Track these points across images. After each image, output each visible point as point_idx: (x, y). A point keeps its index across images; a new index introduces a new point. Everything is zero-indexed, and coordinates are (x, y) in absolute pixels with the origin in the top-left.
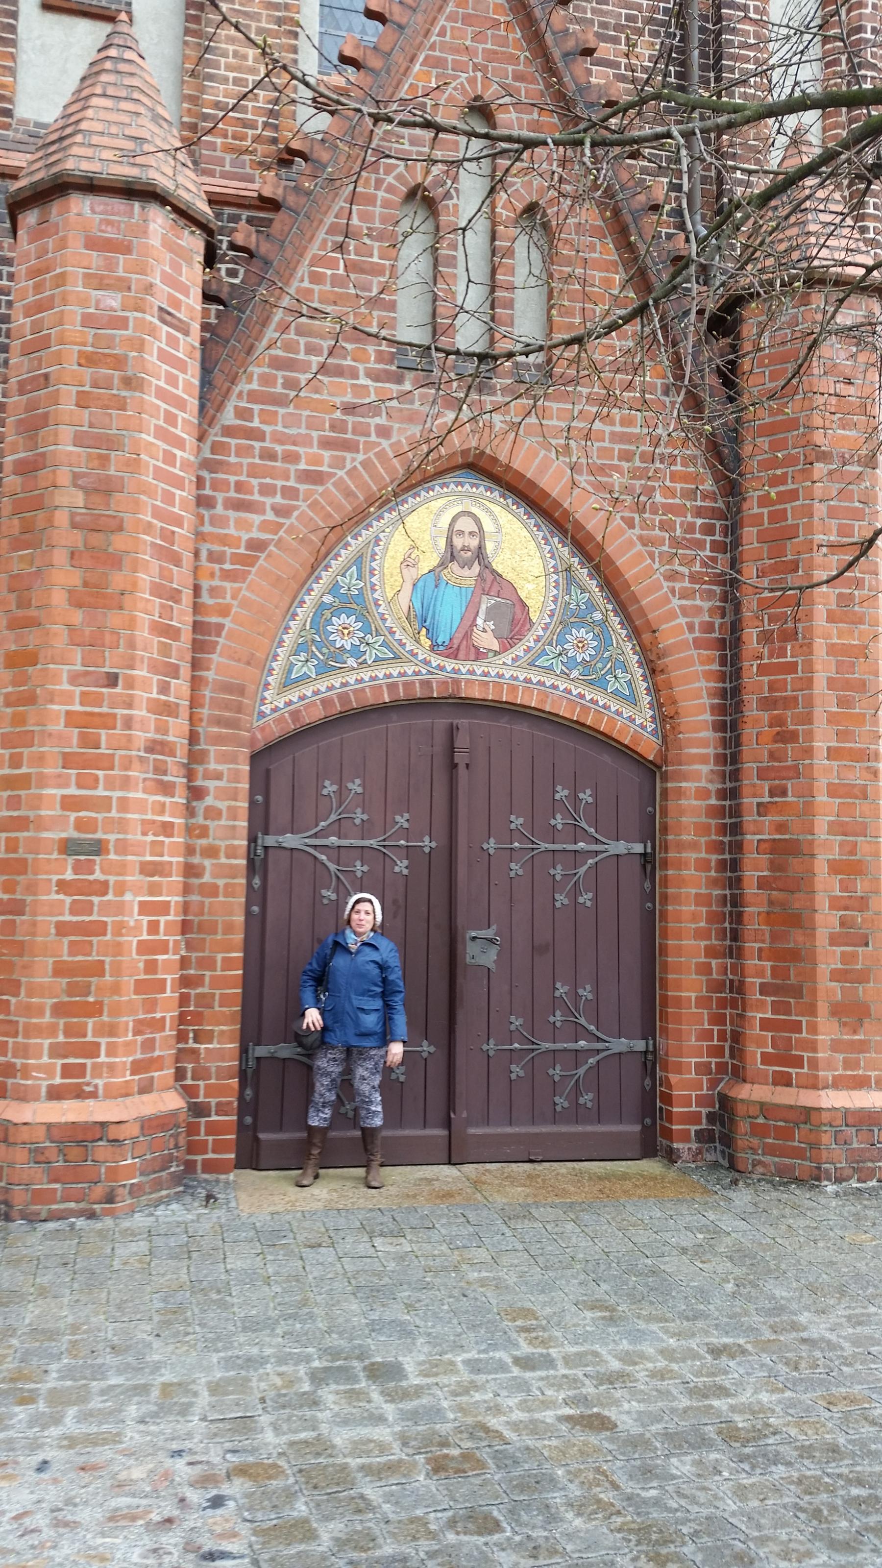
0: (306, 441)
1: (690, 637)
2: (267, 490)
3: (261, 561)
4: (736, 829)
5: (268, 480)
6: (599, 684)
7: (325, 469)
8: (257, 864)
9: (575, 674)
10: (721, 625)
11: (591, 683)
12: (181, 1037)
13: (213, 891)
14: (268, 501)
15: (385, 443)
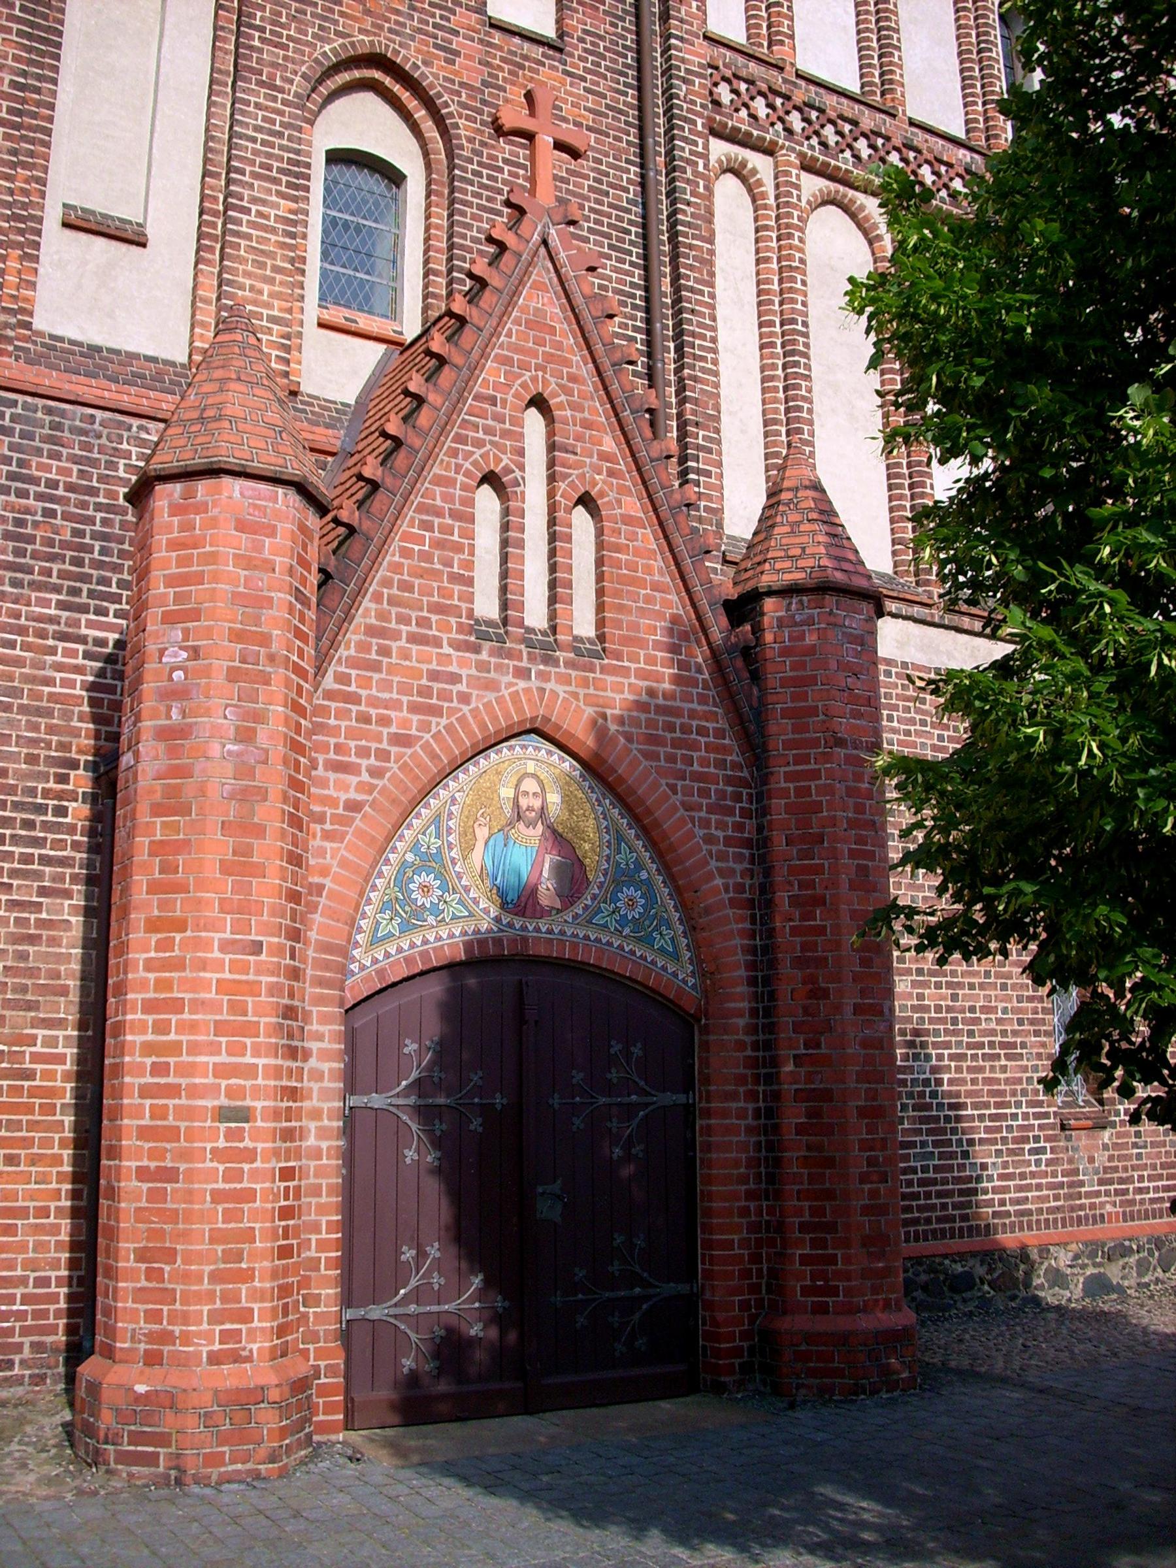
0: (396, 705)
1: (726, 896)
2: (363, 752)
3: (357, 822)
5: (363, 743)
6: (647, 941)
7: (414, 732)
9: (627, 931)
10: (751, 886)
11: (639, 940)
14: (364, 763)
15: (466, 709)
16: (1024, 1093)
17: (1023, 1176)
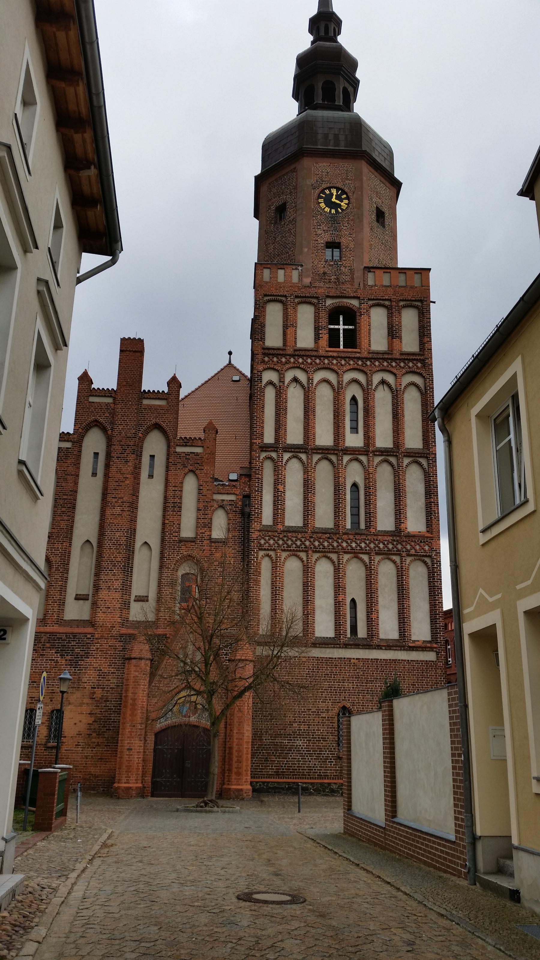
4: (225, 745)
8: (155, 750)
12: (142, 777)
13: (148, 755)
16: (328, 749)
17: (326, 767)
